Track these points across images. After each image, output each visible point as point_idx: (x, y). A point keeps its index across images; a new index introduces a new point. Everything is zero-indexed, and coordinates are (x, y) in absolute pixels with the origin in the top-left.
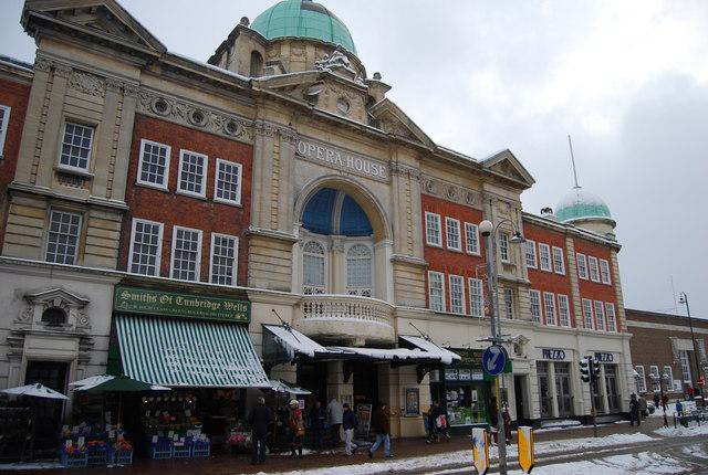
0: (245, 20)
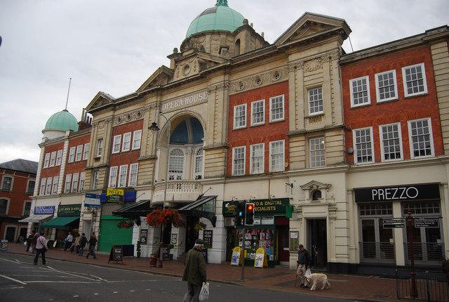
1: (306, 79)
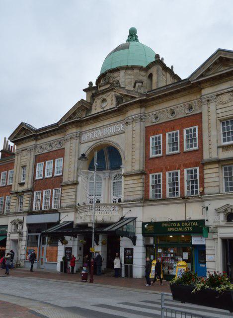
0: (91, 83)
1: (219, 111)
